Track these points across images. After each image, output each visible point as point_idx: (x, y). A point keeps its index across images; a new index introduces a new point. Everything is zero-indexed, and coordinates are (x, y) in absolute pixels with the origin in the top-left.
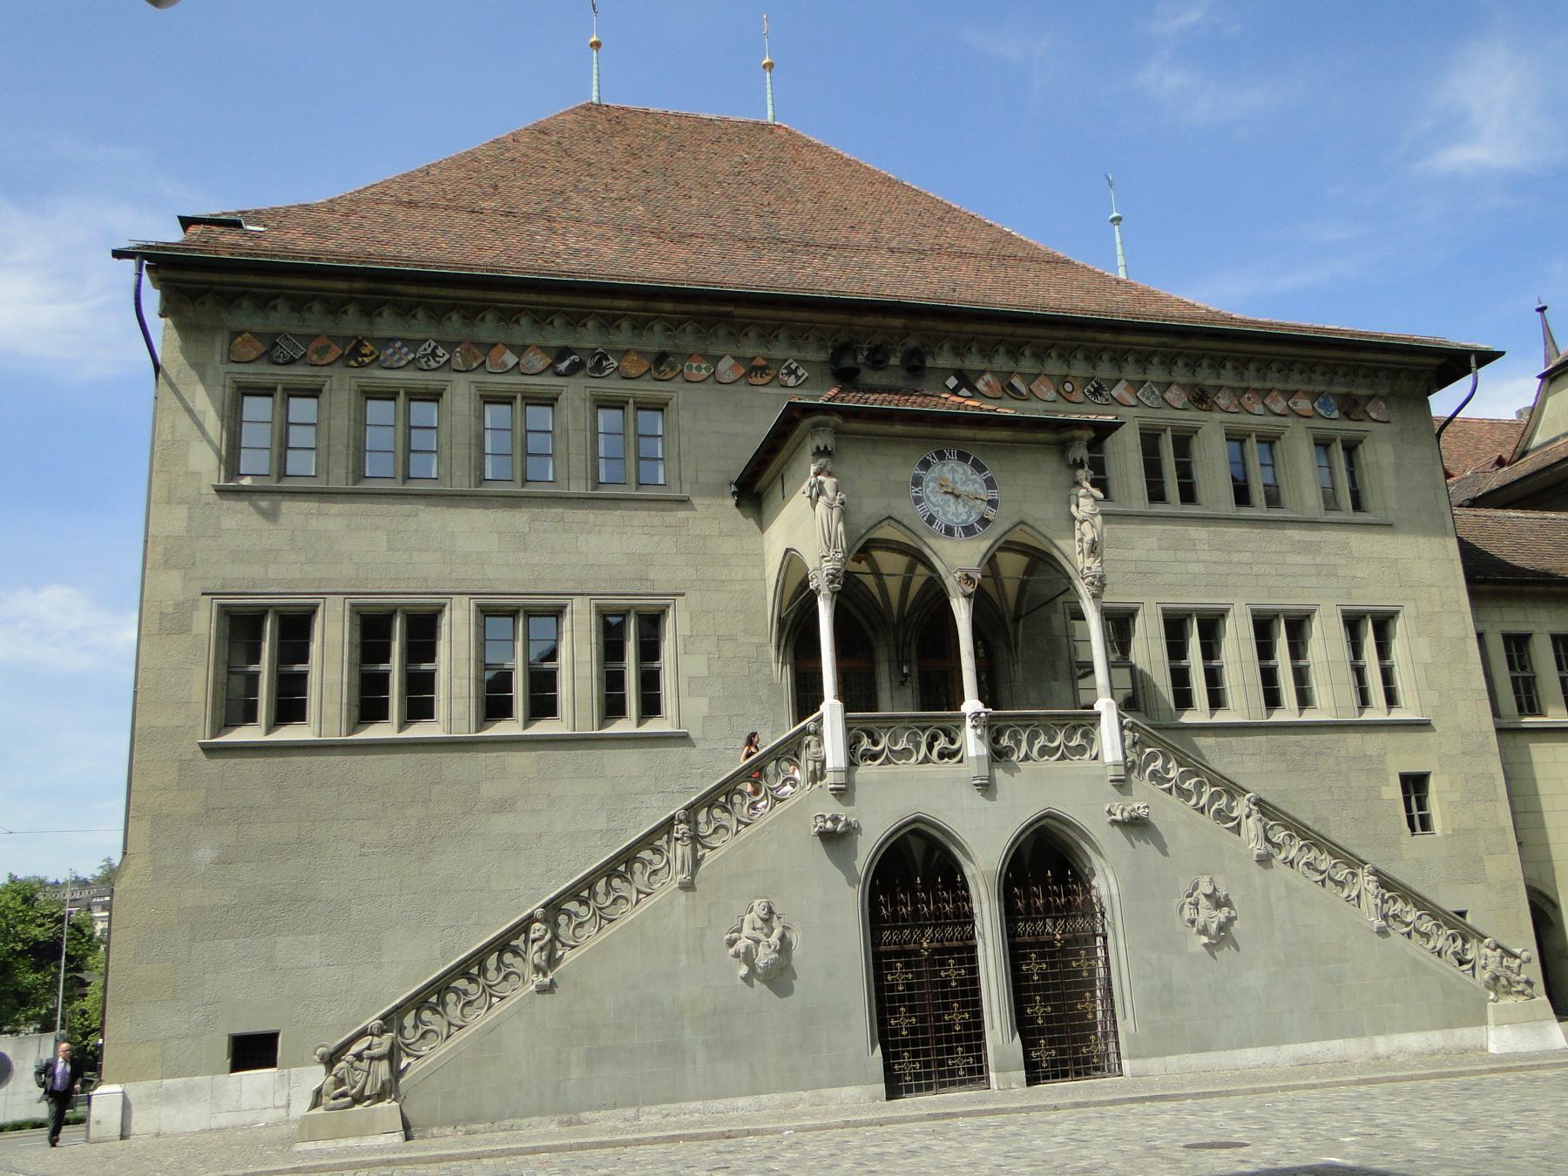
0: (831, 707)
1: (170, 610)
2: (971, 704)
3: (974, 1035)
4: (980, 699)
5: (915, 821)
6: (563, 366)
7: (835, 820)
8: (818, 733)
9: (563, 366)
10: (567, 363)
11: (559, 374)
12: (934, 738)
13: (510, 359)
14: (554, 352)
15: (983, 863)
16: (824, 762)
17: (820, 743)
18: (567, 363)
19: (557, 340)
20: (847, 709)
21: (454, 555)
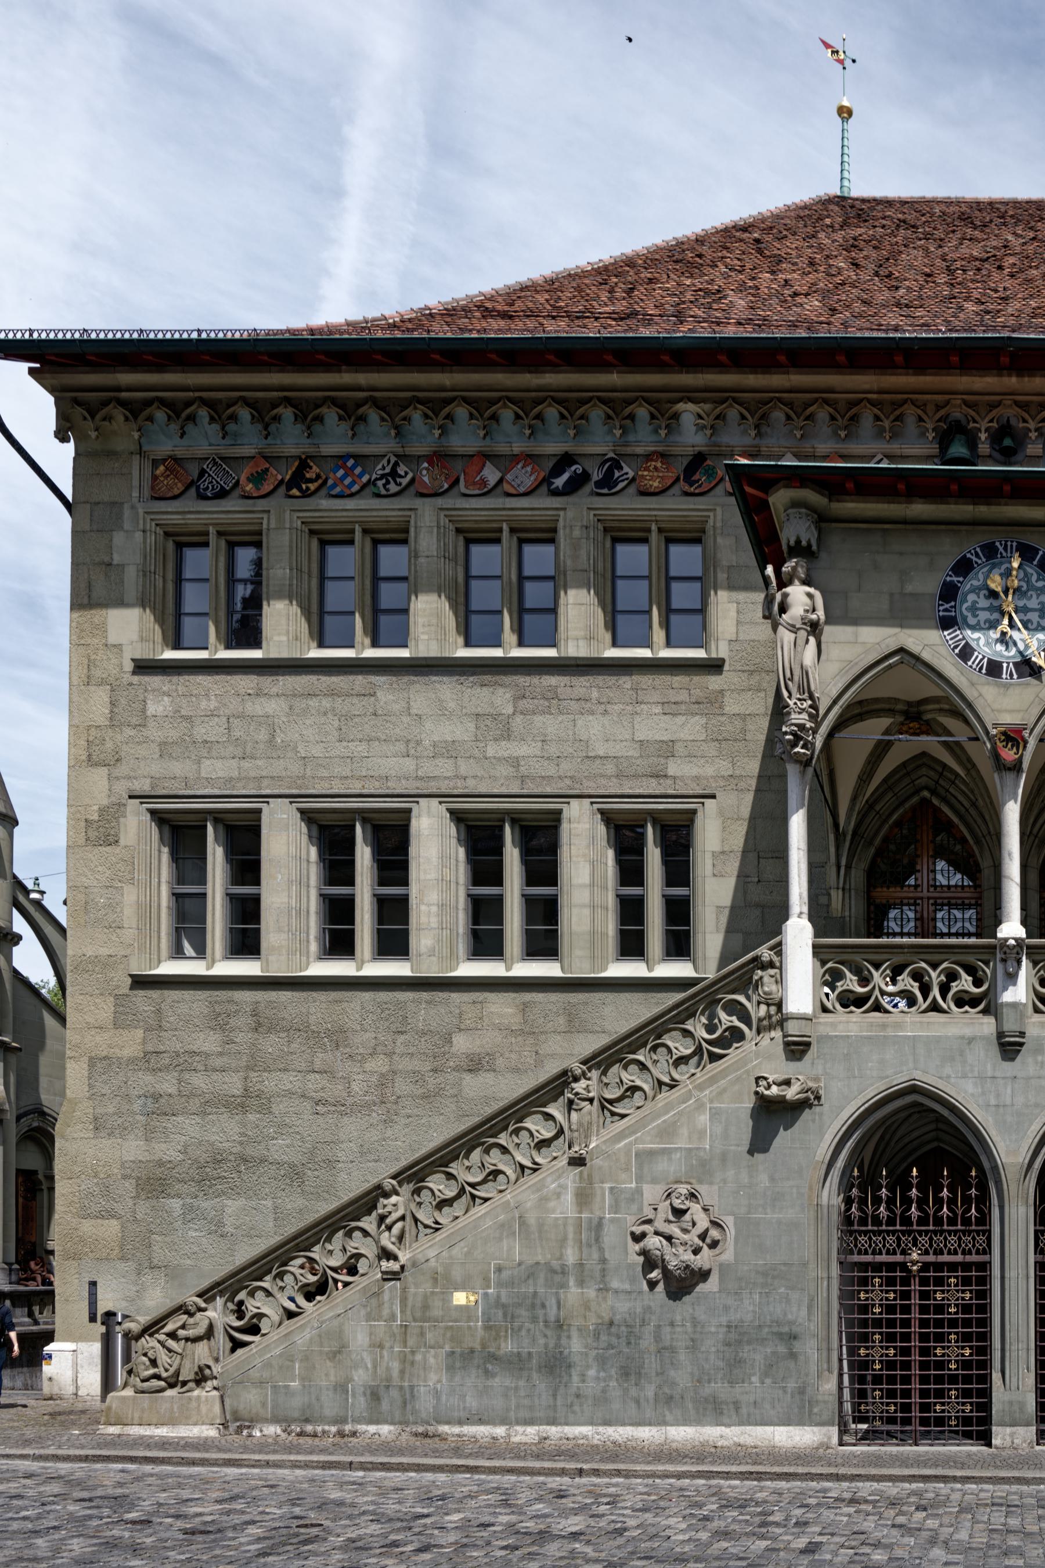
0: (799, 934)
1: (95, 817)
2: (1011, 929)
3: (976, 1382)
4: (1024, 922)
5: (913, 1089)
6: (559, 482)
7: (787, 1083)
8: (776, 965)
9: (559, 482)
10: (565, 476)
11: (555, 493)
12: (952, 976)
13: (491, 474)
14: (551, 464)
15: (1011, 1150)
16: (779, 1005)
17: (780, 981)
18: (565, 476)
19: (553, 447)
20: (817, 935)
21: (426, 739)
